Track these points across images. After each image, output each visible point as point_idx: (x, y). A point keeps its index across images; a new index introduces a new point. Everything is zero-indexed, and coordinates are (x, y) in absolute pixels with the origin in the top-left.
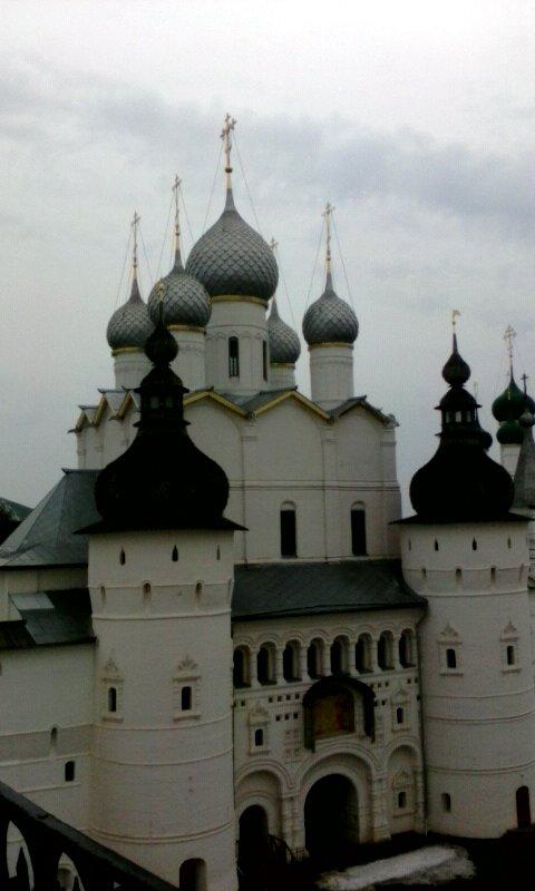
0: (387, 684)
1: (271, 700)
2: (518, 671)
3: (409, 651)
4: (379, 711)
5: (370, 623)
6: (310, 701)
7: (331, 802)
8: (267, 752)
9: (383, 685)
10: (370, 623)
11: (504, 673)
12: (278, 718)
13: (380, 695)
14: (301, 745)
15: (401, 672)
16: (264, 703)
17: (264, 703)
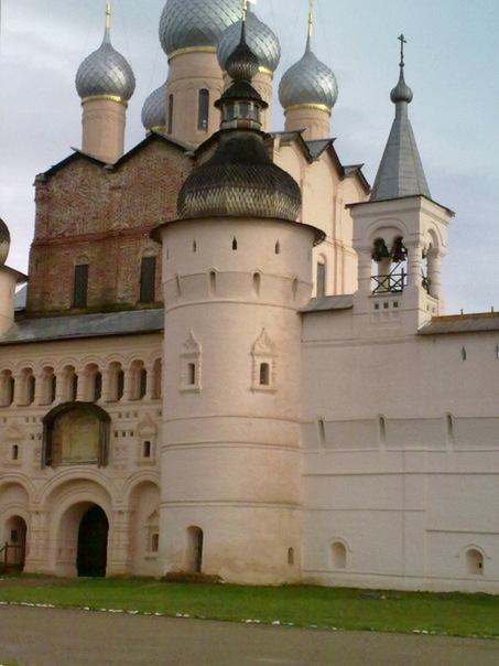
0: (136, 415)
1: (27, 420)
2: (197, 391)
3: (146, 381)
4: (114, 442)
5: (120, 352)
6: (50, 422)
7: (91, 526)
8: (19, 466)
9: (132, 415)
10: (120, 352)
11: (183, 392)
12: (33, 438)
13: (118, 424)
14: (39, 464)
15: (147, 404)
16: (21, 421)
17: (21, 421)
